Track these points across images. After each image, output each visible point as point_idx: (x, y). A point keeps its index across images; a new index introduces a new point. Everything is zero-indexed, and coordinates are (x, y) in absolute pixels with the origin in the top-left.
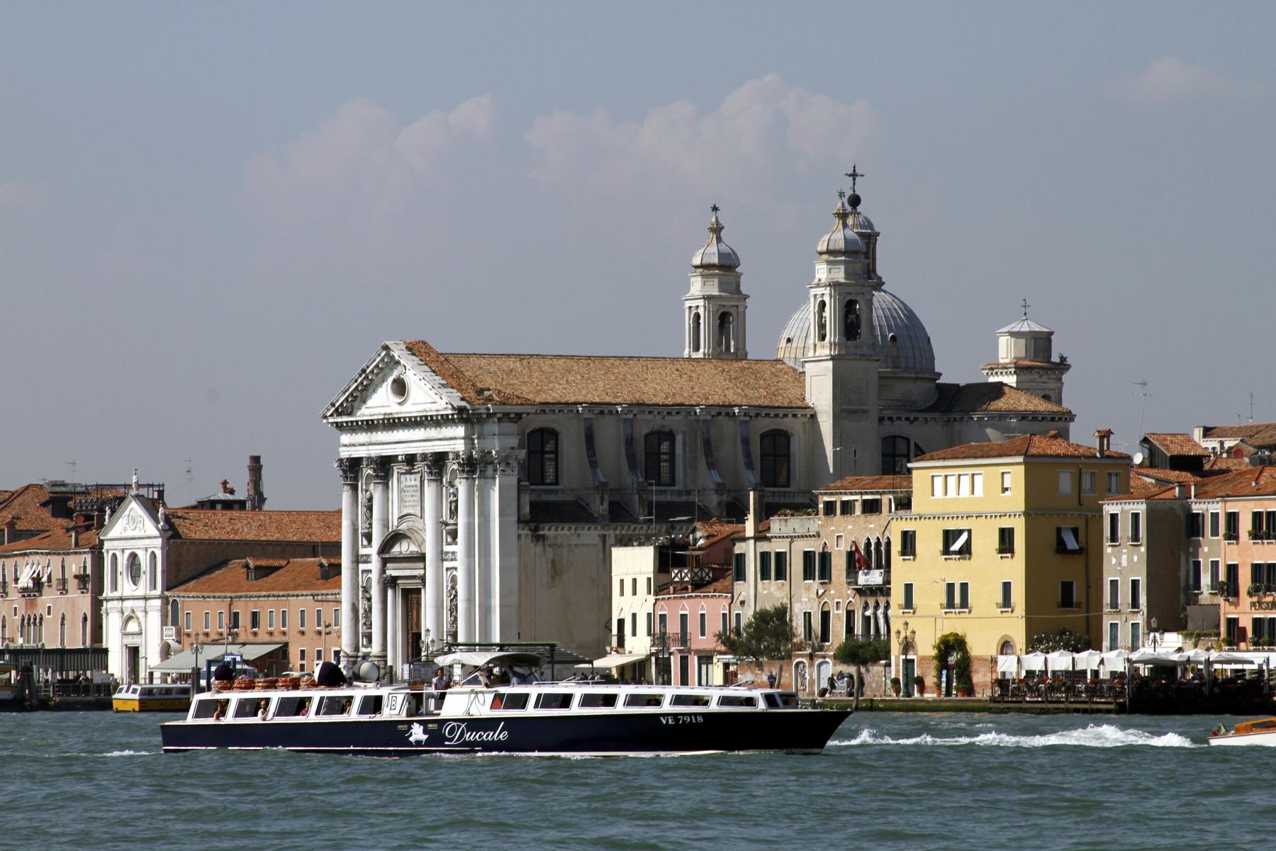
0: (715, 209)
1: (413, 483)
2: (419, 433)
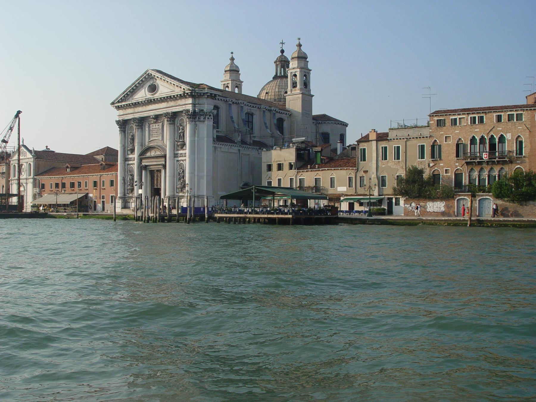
0: (232, 53)
1: (157, 127)
2: (164, 105)
